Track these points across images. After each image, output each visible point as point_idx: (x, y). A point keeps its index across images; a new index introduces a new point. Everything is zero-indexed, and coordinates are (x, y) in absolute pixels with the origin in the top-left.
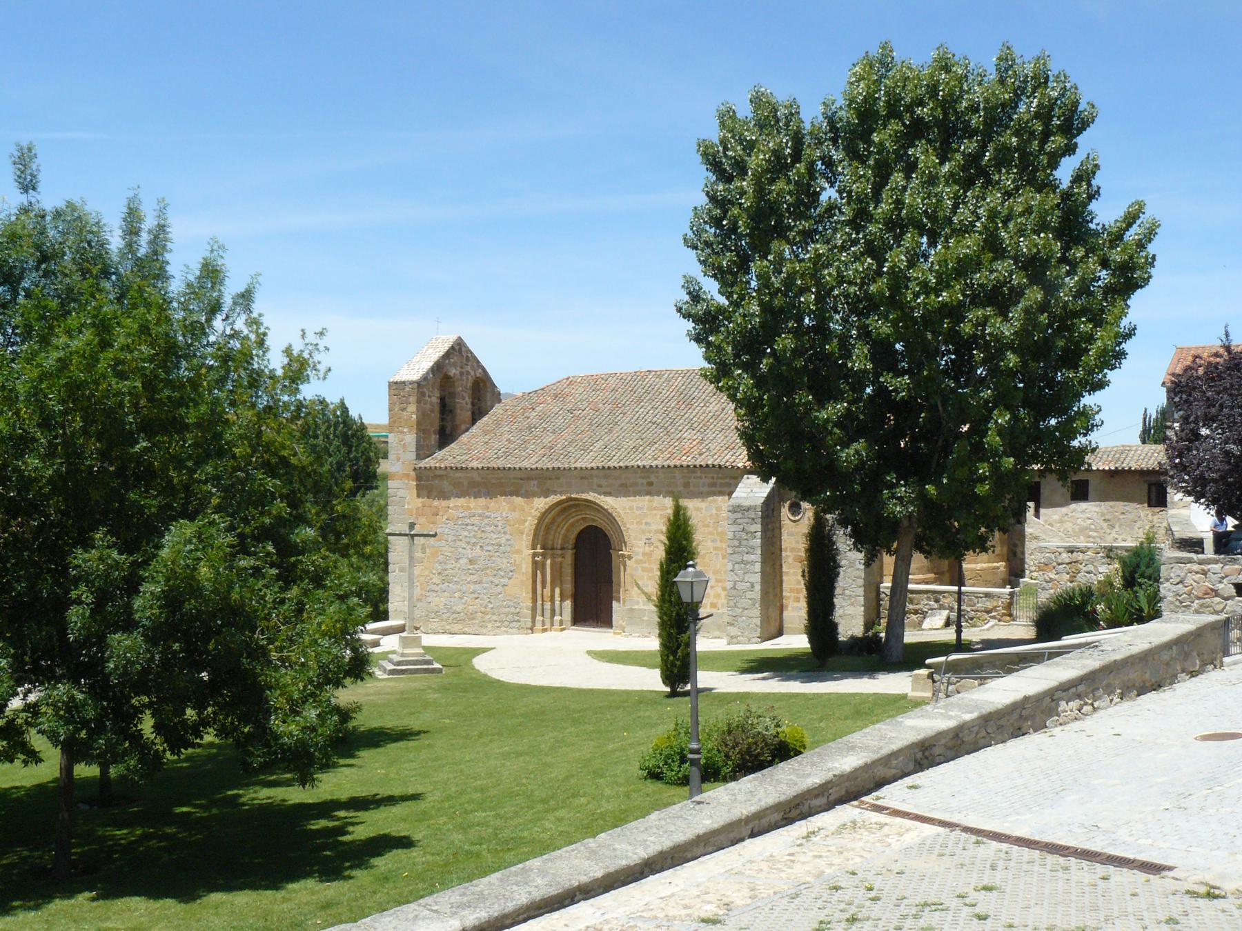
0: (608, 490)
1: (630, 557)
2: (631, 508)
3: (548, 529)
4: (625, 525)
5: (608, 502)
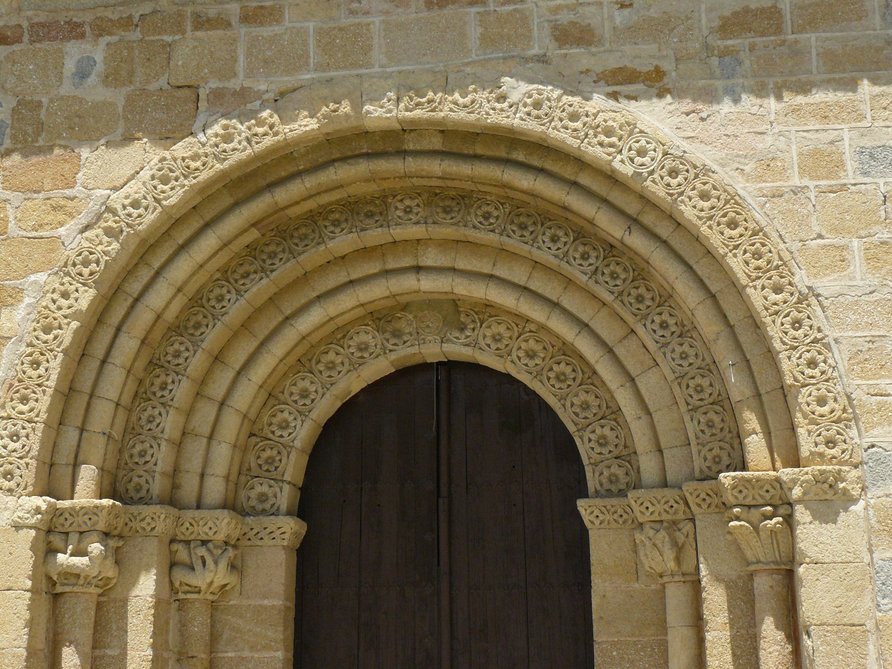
0: (641, 55)
1: (830, 500)
2: (822, 162)
3: (155, 365)
4: (778, 276)
5: (654, 134)
